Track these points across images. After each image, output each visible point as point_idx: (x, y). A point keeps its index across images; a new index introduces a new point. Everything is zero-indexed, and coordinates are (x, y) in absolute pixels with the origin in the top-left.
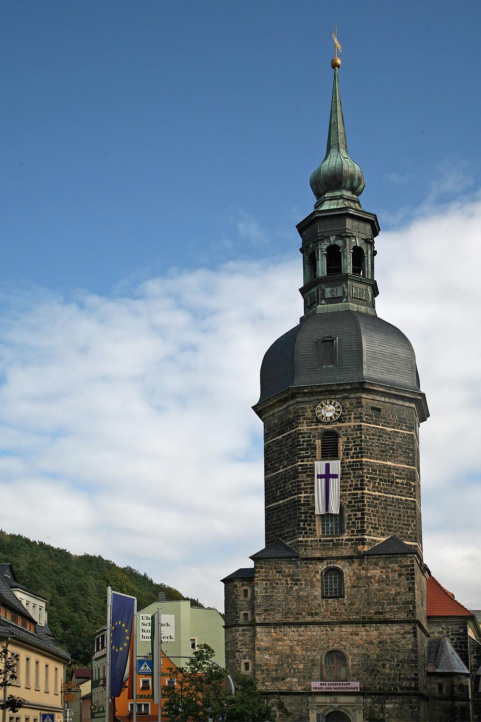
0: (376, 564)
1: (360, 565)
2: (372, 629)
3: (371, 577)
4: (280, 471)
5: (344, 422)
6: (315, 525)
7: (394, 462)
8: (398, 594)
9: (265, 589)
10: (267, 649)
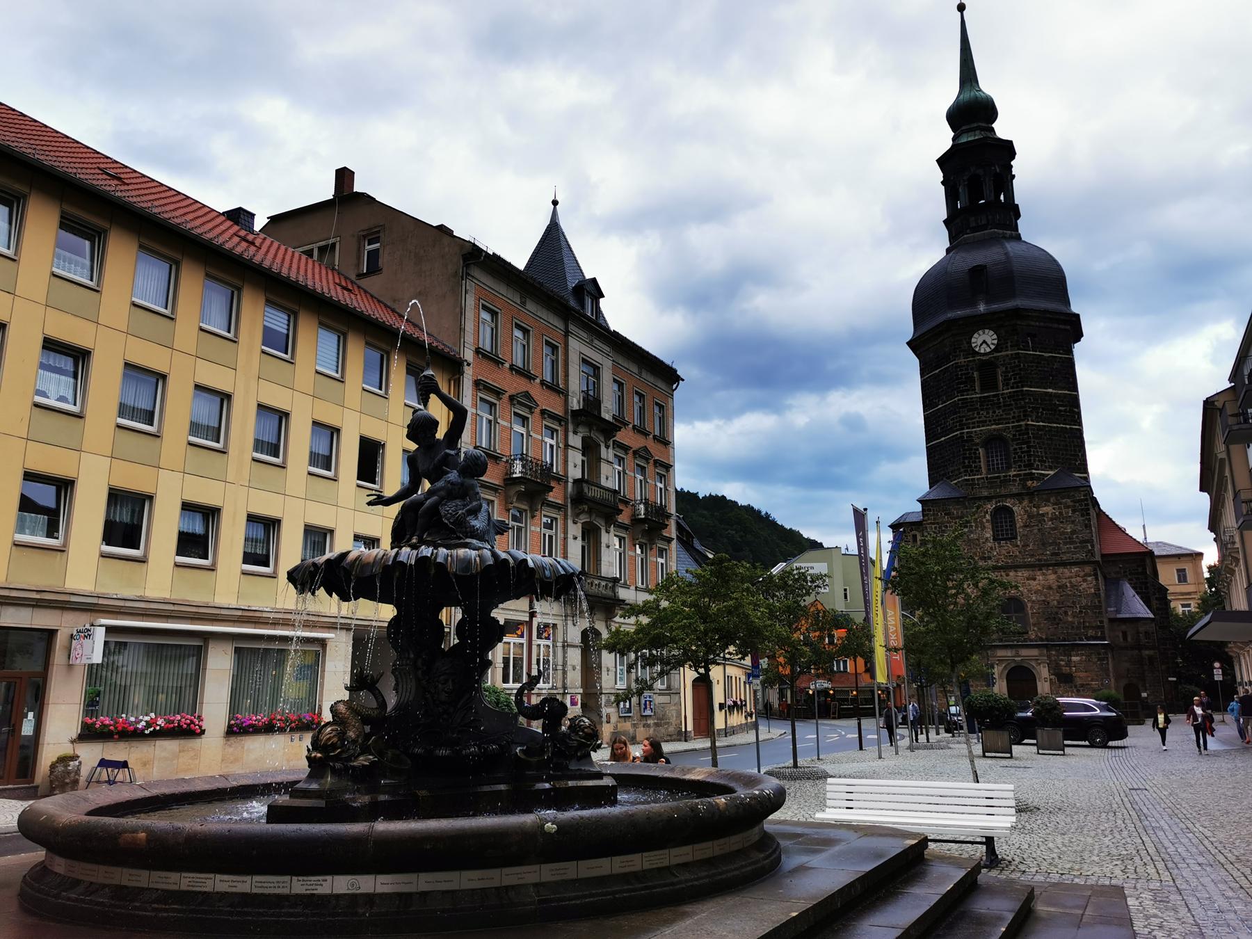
1: (1031, 502)
3: (1043, 515)
8: (1073, 532)
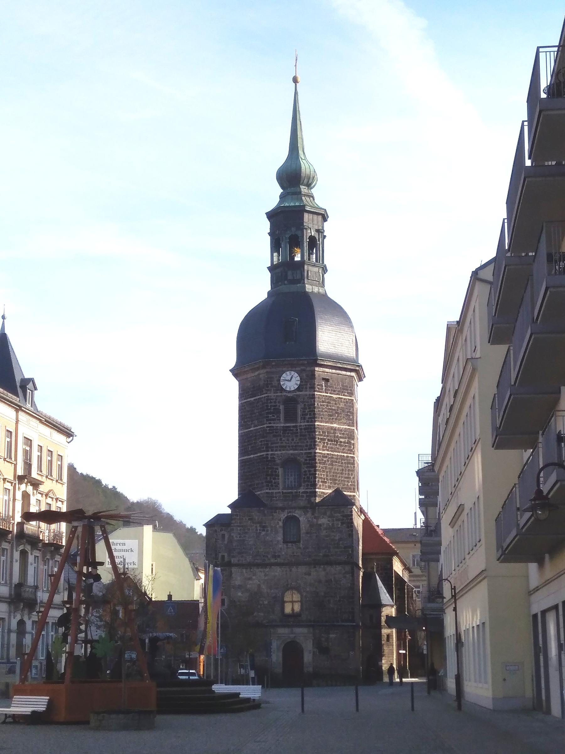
0: (325, 514)
1: (313, 514)
2: (321, 569)
3: (320, 525)
4: (251, 429)
5: (301, 391)
6: (279, 479)
7: (339, 424)
8: (340, 539)
9: (239, 534)
10: (240, 587)
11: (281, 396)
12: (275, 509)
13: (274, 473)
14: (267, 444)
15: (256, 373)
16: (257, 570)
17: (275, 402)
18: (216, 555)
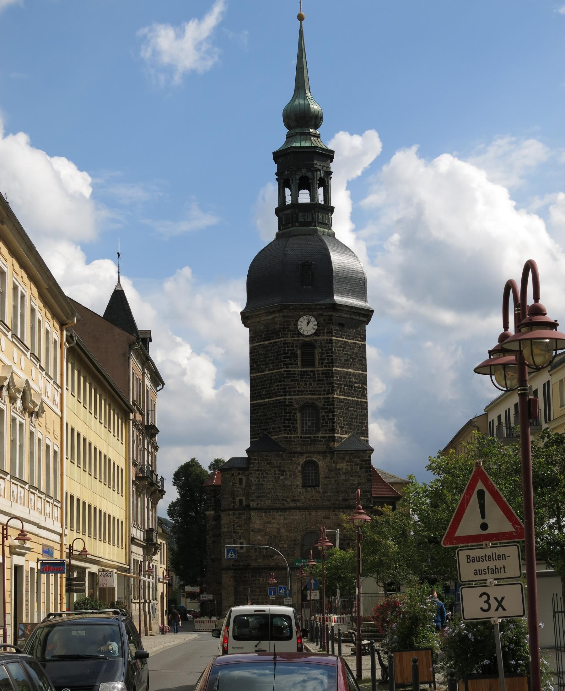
6: (297, 423)
9: (258, 478)
10: (259, 530)
11: (298, 340)
12: (294, 453)
13: (292, 418)
14: (285, 389)
15: (271, 317)
16: (276, 514)
17: (292, 347)
18: (234, 499)
